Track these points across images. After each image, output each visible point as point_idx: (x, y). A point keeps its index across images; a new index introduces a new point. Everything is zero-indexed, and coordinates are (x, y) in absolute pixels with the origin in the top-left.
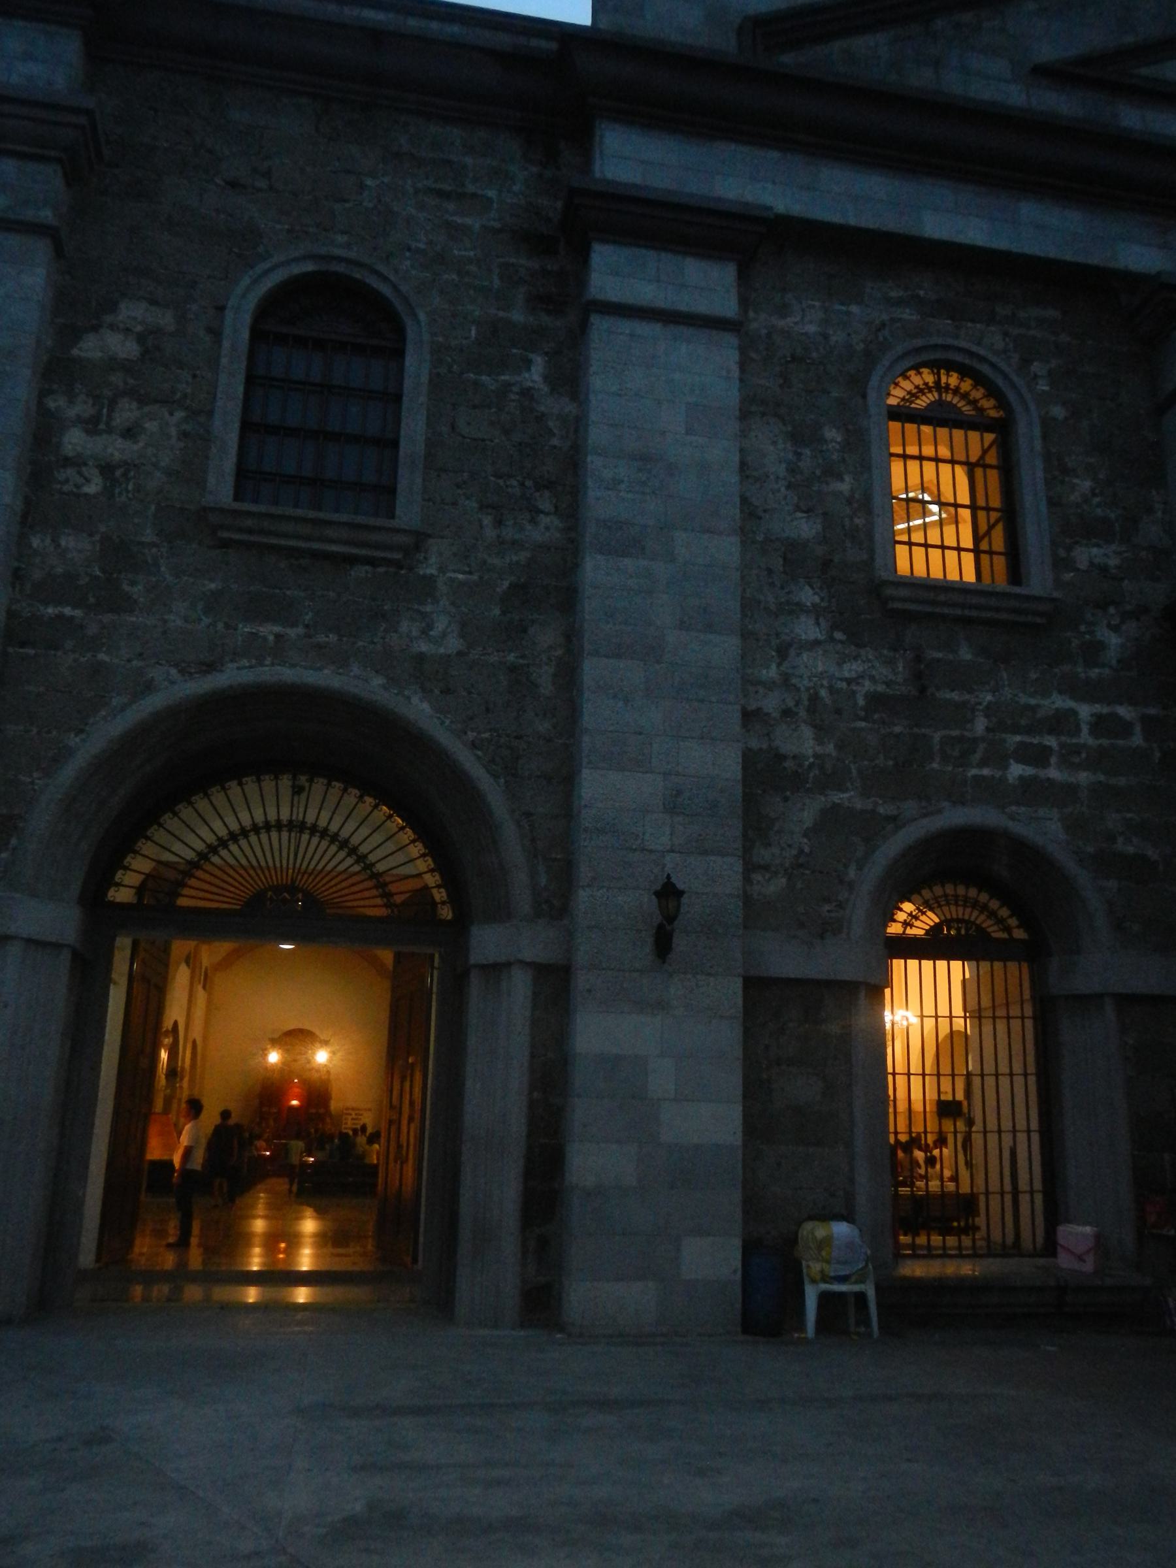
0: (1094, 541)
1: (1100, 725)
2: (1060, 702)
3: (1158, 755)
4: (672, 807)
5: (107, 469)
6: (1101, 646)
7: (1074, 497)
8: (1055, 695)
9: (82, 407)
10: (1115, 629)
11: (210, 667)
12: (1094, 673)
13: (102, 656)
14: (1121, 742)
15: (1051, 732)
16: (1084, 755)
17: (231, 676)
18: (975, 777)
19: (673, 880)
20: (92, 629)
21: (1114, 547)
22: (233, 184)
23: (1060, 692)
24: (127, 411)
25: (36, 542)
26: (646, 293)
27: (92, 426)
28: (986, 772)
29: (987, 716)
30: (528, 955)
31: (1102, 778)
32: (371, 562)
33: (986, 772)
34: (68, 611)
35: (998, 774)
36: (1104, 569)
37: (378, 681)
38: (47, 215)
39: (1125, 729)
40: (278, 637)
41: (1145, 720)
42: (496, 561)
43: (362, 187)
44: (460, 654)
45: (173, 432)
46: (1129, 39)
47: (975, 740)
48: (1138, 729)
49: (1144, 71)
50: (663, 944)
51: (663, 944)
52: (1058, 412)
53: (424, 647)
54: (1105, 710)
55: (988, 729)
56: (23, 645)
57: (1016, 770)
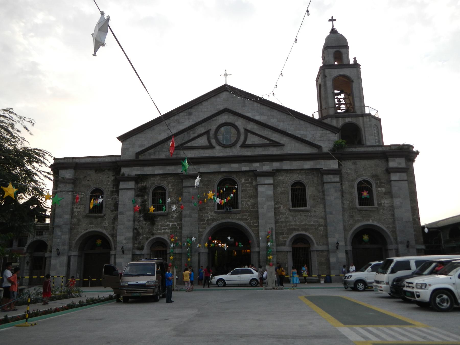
1: (172, 225)
2: (168, 223)
4: (125, 239)
5: (78, 212)
6: (173, 216)
9: (75, 206)
10: (175, 214)
11: (87, 230)
12: (172, 220)
13: (78, 230)
15: (167, 226)
17: (89, 230)
20: (77, 228)
22: (88, 180)
23: (168, 222)
24: (79, 206)
25: (72, 220)
26: (125, 186)
27: (76, 208)
28: (159, 231)
29: (160, 225)
30: (114, 254)
32: (100, 218)
33: (159, 231)
34: (75, 226)
35: (161, 231)
37: (101, 229)
38: (71, 190)
40: (92, 226)
41: (177, 224)
42: (112, 216)
43: (100, 178)
44: (108, 226)
45: (83, 207)
46: (184, 142)
47: (159, 228)
49: (185, 146)
50: (123, 252)
51: (123, 252)
52: (171, 190)
53: (105, 225)
54: (173, 223)
55: (160, 227)
56: (72, 229)
57: (163, 231)
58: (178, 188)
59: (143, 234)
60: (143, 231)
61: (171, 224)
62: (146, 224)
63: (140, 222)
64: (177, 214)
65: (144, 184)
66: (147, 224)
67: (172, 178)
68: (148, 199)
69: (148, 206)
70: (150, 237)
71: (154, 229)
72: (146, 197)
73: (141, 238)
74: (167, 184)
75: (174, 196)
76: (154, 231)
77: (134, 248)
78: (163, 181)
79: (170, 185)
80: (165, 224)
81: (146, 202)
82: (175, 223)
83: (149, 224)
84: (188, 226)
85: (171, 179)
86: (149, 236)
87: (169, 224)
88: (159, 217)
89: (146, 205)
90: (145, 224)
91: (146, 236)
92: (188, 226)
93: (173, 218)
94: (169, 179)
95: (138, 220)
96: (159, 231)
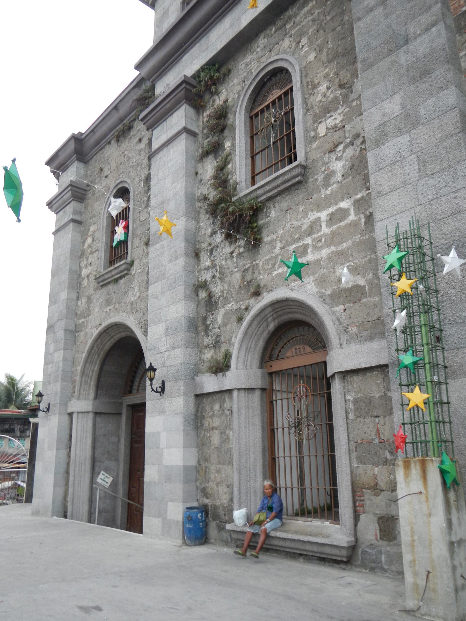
0: (328, 115)
1: (332, 219)
2: (312, 216)
3: (363, 220)
7: (319, 98)
8: (310, 213)
14: (343, 224)
16: (323, 240)
18: (276, 275)
19: (153, 365)
21: (339, 111)
29: (281, 242)
31: (333, 248)
36: (335, 128)
39: (344, 213)
47: (276, 257)
48: (352, 212)
54: (332, 210)
58: (339, 28)
59: (226, 301)
60: (226, 286)
61: (324, 215)
62: (232, 253)
63: (214, 253)
64: (350, 152)
65: (219, 101)
66: (237, 251)
67: (311, 5)
68: (233, 146)
69: (234, 178)
70: (247, 309)
71: (261, 264)
72: (227, 144)
73: (220, 320)
74: (294, 44)
75: (326, 76)
76: (261, 277)
77: (196, 372)
78: (277, 43)
79: (304, 41)
80: (301, 226)
81: (229, 164)
82: (344, 205)
83: (241, 250)
84: (405, 183)
85: (310, 12)
86: (246, 303)
87: (318, 219)
88: (274, 207)
89: (230, 176)
90: (229, 256)
91: (235, 307)
92: (405, 183)
93: (333, 180)
94: (298, 18)
95: (210, 248)
96: (278, 269)
